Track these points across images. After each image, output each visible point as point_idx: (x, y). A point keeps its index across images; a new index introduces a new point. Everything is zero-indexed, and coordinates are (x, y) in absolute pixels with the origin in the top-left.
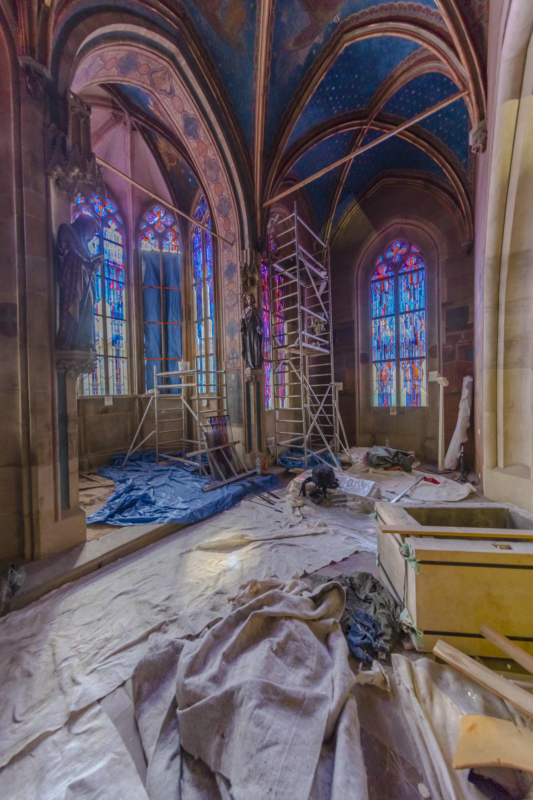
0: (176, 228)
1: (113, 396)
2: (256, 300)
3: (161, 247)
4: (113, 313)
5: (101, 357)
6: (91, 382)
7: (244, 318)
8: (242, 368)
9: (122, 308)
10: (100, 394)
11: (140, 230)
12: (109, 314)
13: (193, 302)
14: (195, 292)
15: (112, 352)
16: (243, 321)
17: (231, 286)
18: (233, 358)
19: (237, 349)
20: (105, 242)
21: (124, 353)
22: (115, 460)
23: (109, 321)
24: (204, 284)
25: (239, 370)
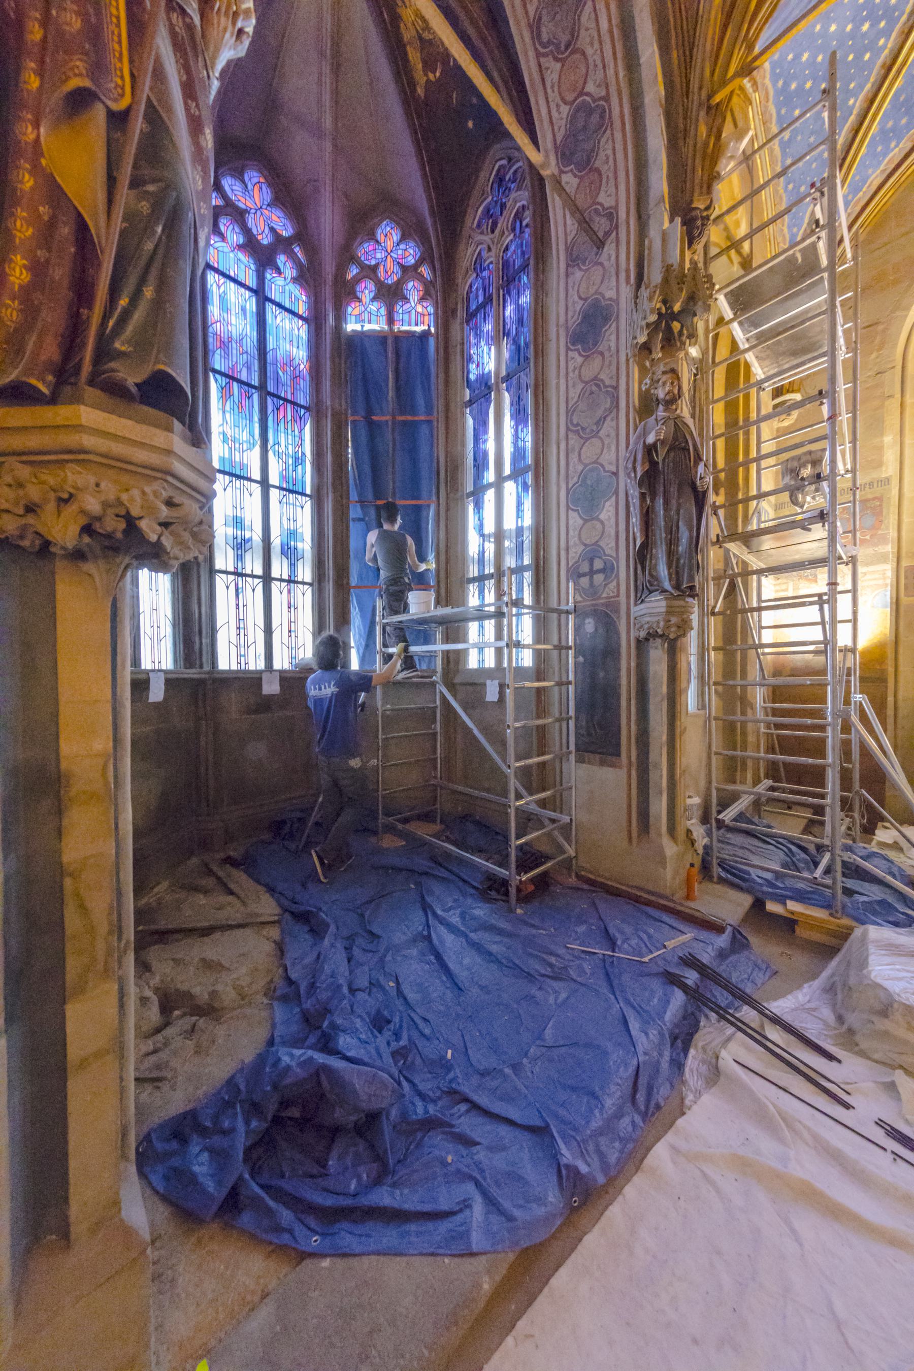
0: (425, 270)
1: (281, 672)
2: (685, 387)
3: (391, 320)
4: (284, 478)
5: (257, 581)
6: (234, 639)
7: (651, 439)
8: (623, 599)
9: (303, 469)
10: (252, 667)
11: (345, 283)
12: (274, 479)
13: (463, 445)
14: (470, 421)
15: (279, 568)
16: (650, 450)
17: (593, 367)
18: (592, 573)
19: (608, 545)
20: (270, 307)
21: (305, 572)
22: (284, 822)
23: (274, 494)
24: (498, 391)
25: (613, 606)
